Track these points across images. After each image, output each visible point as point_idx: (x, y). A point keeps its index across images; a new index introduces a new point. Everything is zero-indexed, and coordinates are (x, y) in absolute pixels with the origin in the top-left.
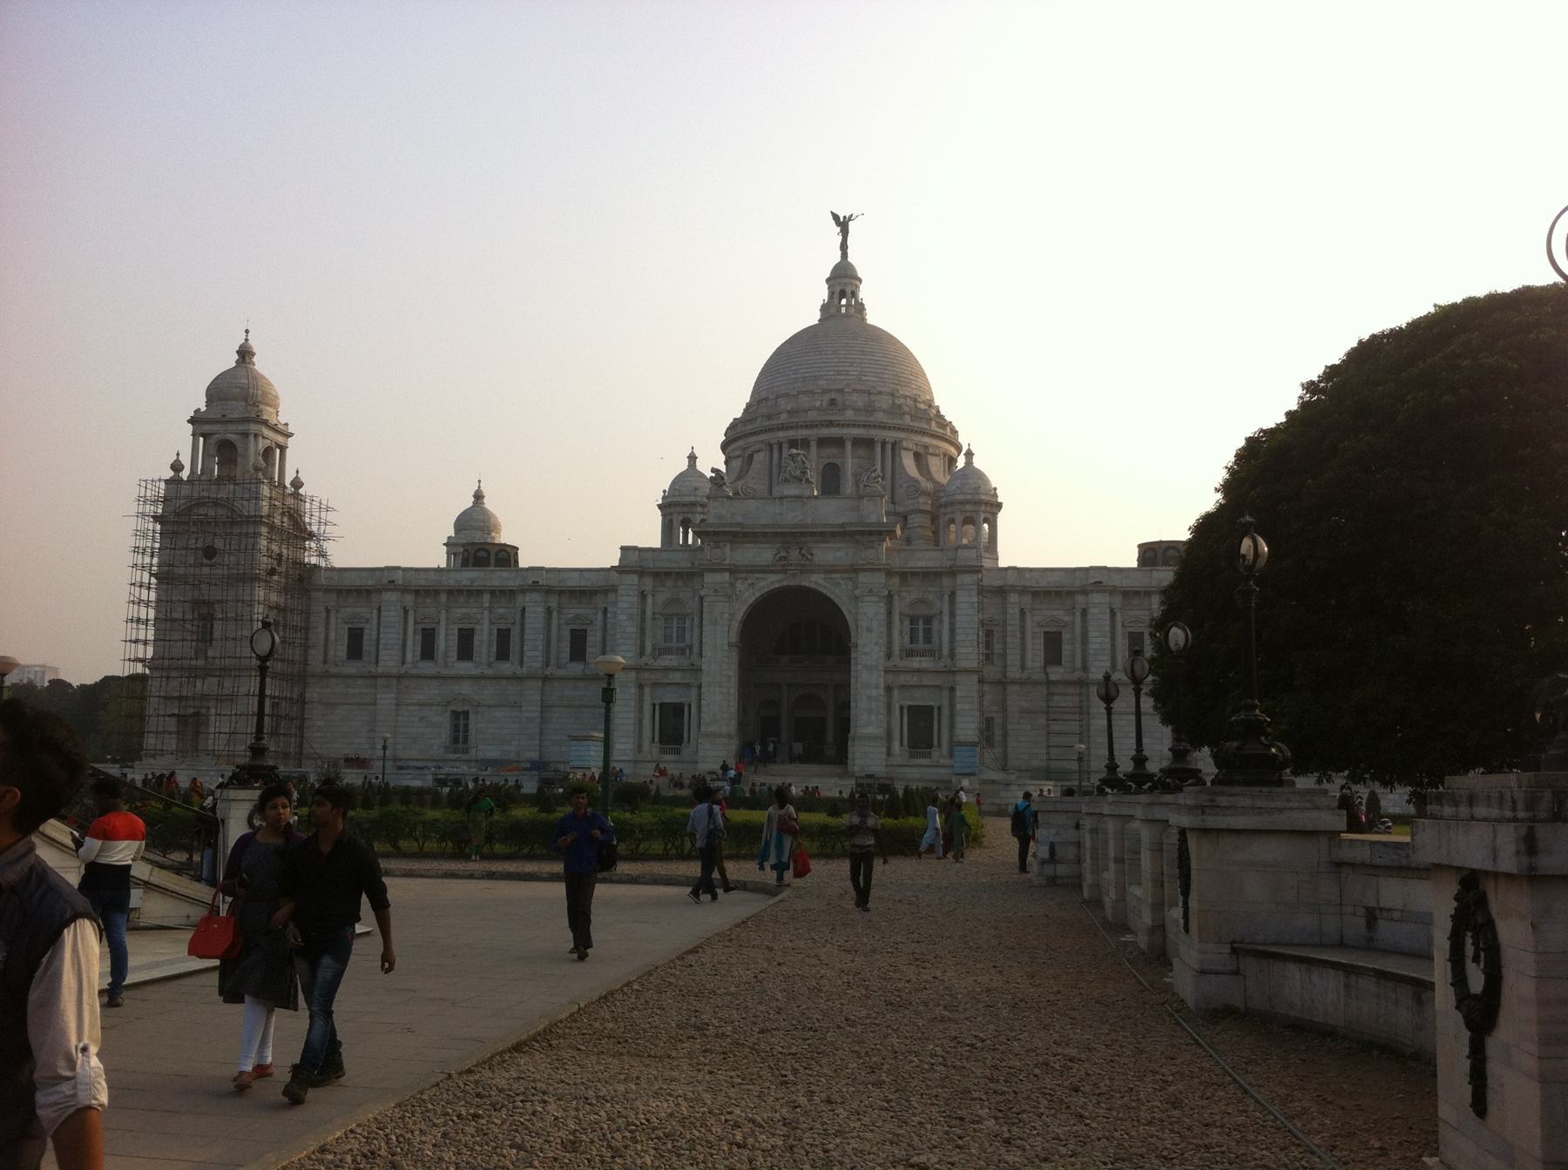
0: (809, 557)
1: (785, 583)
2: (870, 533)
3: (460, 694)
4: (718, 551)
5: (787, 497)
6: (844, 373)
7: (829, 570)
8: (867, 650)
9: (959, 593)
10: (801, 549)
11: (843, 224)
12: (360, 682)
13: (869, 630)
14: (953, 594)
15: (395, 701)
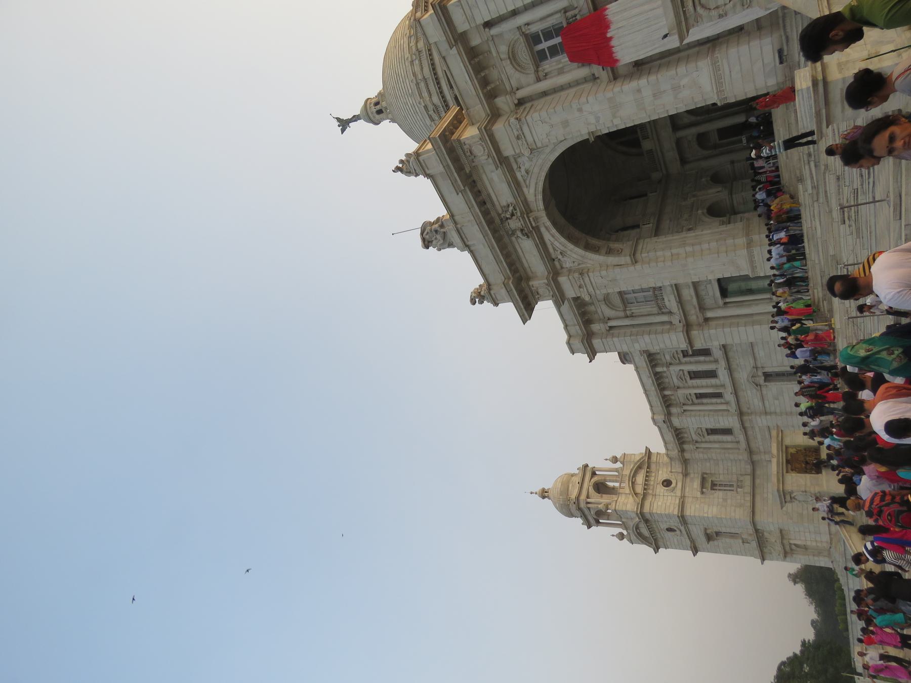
0: (511, 208)
1: (549, 224)
2: (456, 160)
3: (748, 381)
4: (541, 291)
5: (464, 243)
6: (414, 108)
7: (516, 186)
8: (592, 119)
9: (480, 21)
10: (507, 219)
11: (344, 124)
12: (750, 433)
13: (566, 124)
14: (488, 25)
15: (763, 417)
